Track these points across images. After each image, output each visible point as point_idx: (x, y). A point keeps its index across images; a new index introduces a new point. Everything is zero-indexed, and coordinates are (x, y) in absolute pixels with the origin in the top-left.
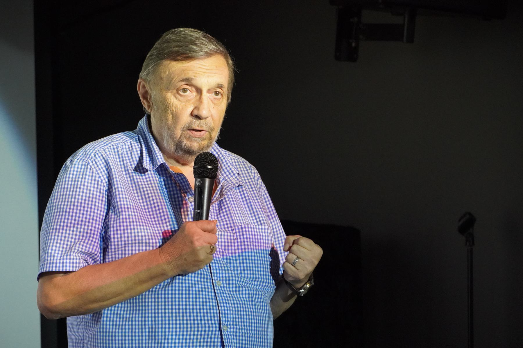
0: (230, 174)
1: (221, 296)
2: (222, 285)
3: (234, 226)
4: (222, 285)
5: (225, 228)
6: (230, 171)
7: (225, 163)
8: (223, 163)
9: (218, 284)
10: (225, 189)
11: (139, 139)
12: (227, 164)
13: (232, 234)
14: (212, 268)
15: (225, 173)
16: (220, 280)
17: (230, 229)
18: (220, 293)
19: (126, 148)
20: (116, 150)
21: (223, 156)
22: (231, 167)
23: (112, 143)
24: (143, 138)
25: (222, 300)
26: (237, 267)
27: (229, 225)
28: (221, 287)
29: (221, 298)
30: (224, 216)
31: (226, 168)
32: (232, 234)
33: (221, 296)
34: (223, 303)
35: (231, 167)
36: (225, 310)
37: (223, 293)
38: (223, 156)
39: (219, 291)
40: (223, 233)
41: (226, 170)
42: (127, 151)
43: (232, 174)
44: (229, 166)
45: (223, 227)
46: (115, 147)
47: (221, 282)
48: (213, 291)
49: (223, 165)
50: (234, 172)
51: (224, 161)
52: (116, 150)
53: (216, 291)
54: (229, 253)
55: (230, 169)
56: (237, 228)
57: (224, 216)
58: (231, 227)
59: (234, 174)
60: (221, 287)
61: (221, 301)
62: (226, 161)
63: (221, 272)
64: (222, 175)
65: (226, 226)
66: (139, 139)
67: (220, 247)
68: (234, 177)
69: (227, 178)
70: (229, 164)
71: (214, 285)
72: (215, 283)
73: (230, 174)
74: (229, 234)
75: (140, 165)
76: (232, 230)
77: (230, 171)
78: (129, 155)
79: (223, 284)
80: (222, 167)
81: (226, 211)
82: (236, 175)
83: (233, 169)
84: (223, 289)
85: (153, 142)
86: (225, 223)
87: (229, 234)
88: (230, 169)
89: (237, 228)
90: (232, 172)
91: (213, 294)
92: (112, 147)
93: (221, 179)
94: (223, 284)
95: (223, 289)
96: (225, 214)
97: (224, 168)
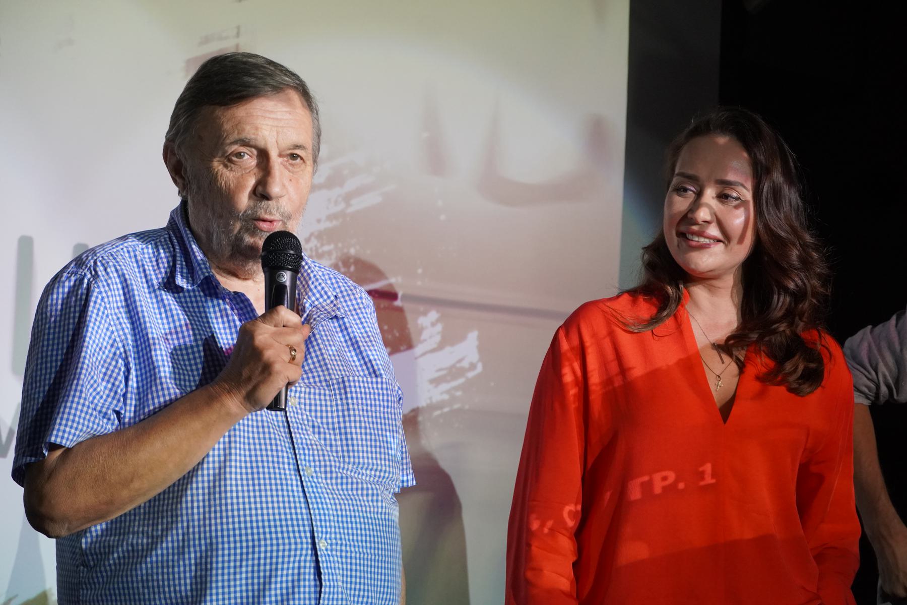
0: (322, 296)
1: (313, 492)
2: (314, 475)
3: (331, 379)
4: (314, 475)
5: (315, 382)
6: (323, 292)
7: (313, 279)
8: (310, 278)
9: (308, 472)
10: (315, 319)
11: (170, 238)
12: (317, 280)
13: (327, 392)
14: (296, 446)
15: (314, 295)
16: (310, 466)
17: (324, 384)
18: (312, 487)
19: (148, 253)
20: (132, 254)
21: (309, 268)
22: (323, 285)
23: (126, 245)
24: (176, 237)
25: (315, 497)
26: (336, 446)
27: (322, 378)
28: (312, 477)
29: (312, 495)
30: (314, 363)
31: (316, 287)
32: (327, 392)
33: (313, 492)
34: (317, 503)
35: (323, 285)
36: (320, 514)
37: (316, 487)
38: (309, 268)
39: (309, 484)
40: (312, 391)
41: (315, 291)
42: (150, 258)
43: (325, 297)
44: (320, 284)
45: (312, 380)
46: (130, 249)
47: (313, 469)
48: (299, 483)
49: (310, 283)
50: (329, 294)
51: (312, 275)
52: (132, 254)
53: (304, 484)
54: (322, 423)
55: (323, 288)
56: (335, 381)
57: (314, 363)
58: (326, 381)
59: (329, 297)
60: (312, 477)
61: (314, 500)
62: (315, 276)
63: (311, 452)
64: (309, 298)
65: (317, 379)
66: (170, 238)
67: (308, 413)
68: (328, 301)
69: (316, 303)
70: (320, 281)
71: (302, 473)
72: (303, 470)
73: (322, 296)
74: (322, 392)
75: (171, 280)
76: (327, 386)
77: (323, 292)
78: (155, 263)
79: (316, 472)
80: (308, 286)
81: (317, 356)
82: (332, 298)
83: (326, 289)
84: (315, 480)
85: (194, 246)
86: (315, 374)
87: (322, 392)
88: (323, 288)
89: (335, 381)
90: (326, 293)
91: (300, 489)
92: (125, 249)
93: (307, 305)
94: (316, 472)
95: (315, 480)
96: (315, 360)
97: (312, 287)
